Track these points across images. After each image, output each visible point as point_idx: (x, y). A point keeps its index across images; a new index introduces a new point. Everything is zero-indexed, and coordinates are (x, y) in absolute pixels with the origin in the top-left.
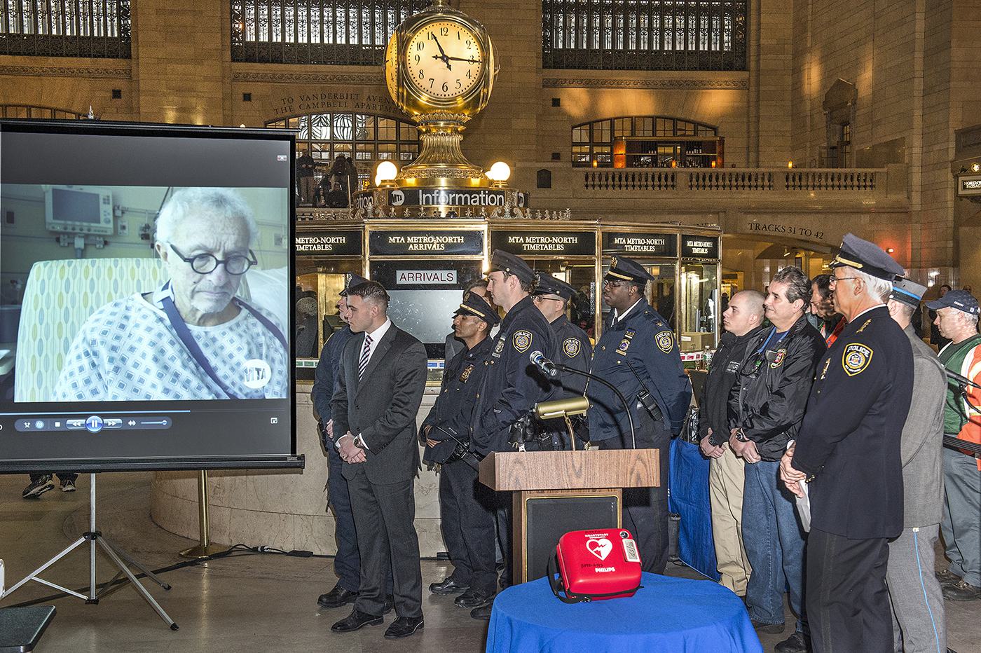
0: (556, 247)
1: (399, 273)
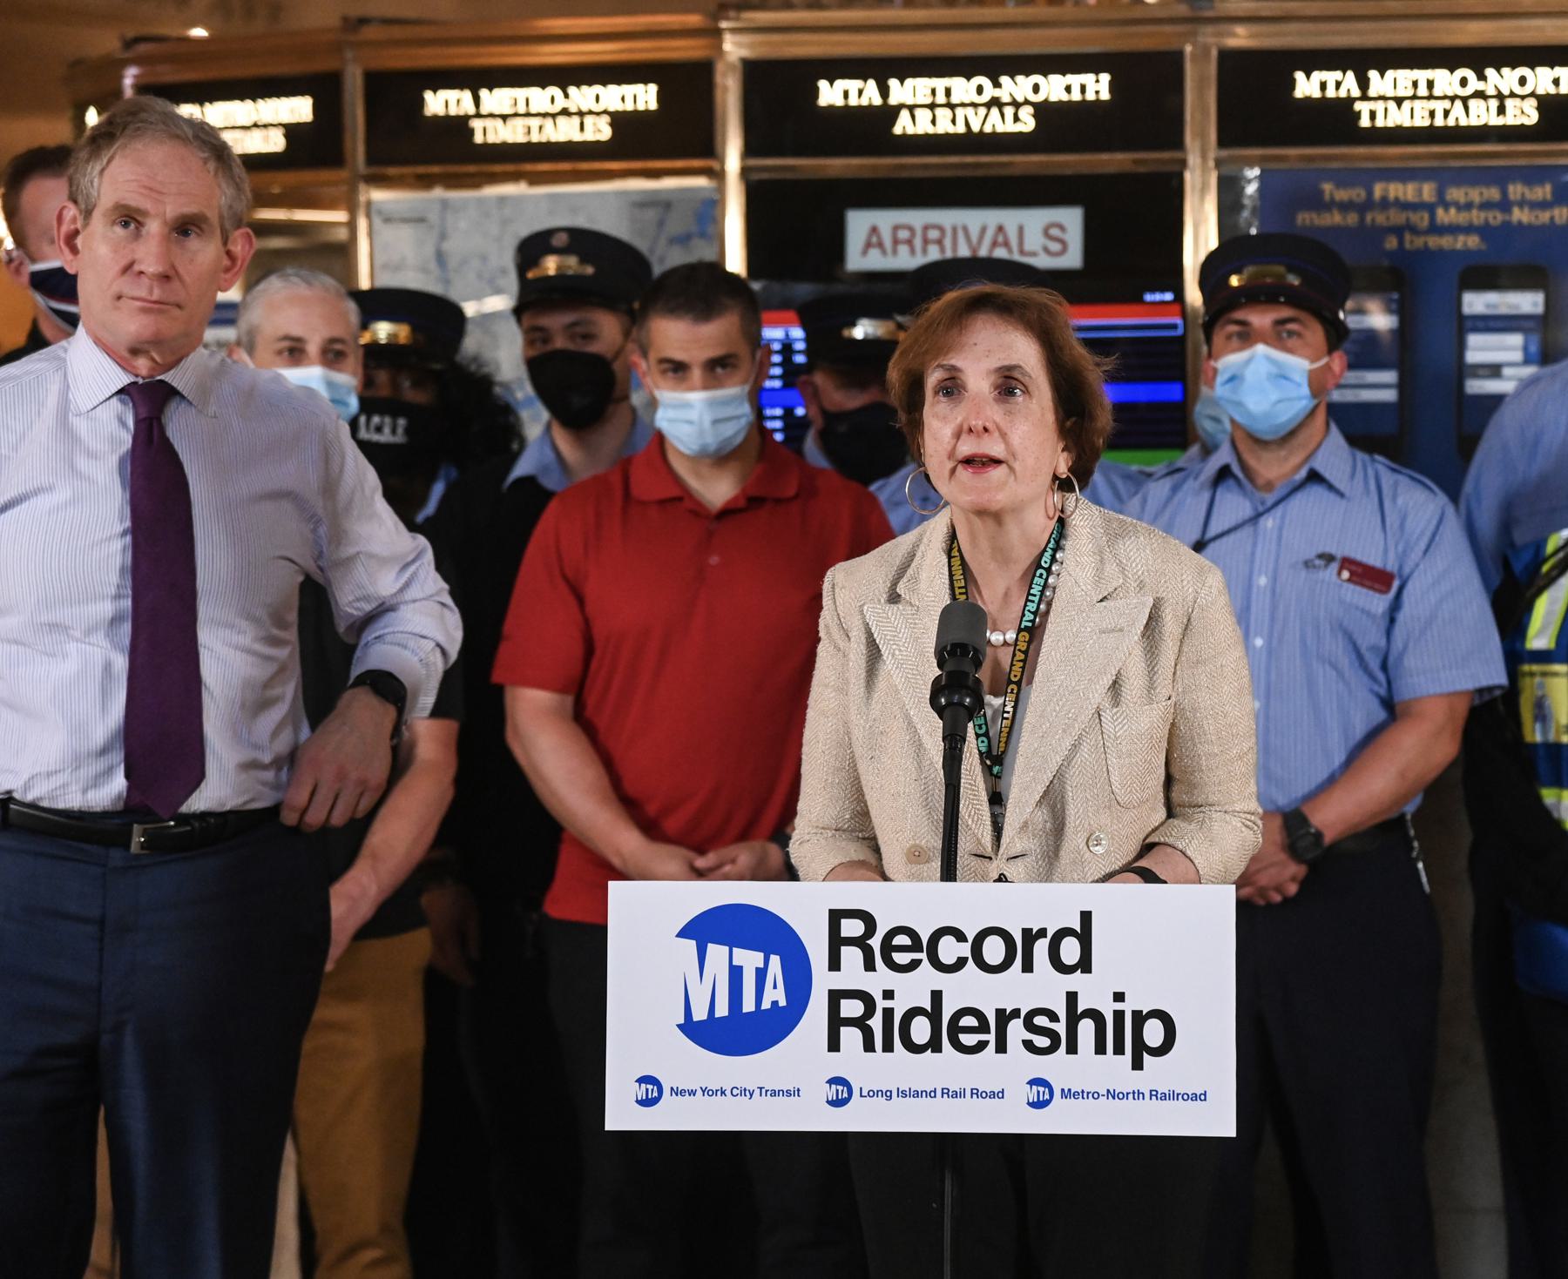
0: (1501, 110)
1: (859, 223)
